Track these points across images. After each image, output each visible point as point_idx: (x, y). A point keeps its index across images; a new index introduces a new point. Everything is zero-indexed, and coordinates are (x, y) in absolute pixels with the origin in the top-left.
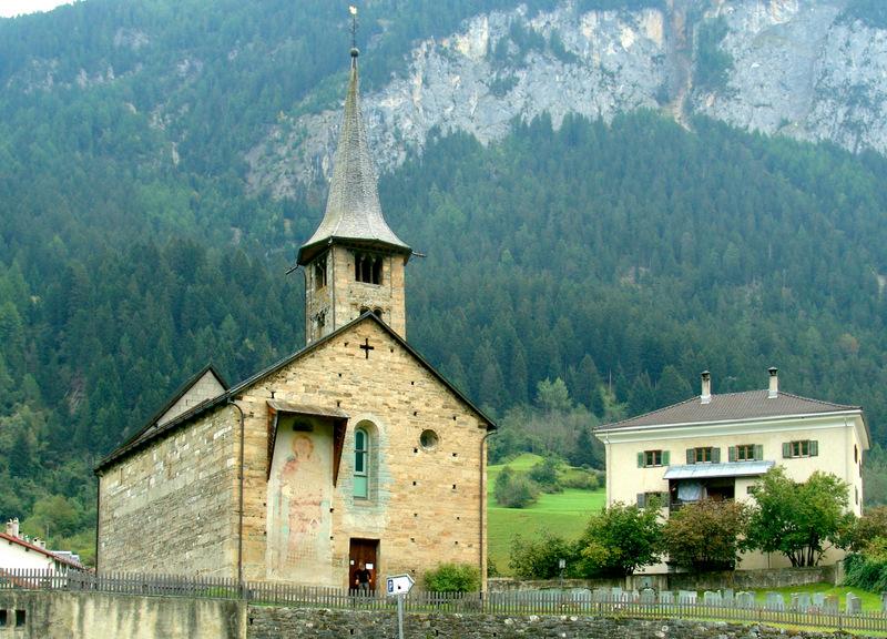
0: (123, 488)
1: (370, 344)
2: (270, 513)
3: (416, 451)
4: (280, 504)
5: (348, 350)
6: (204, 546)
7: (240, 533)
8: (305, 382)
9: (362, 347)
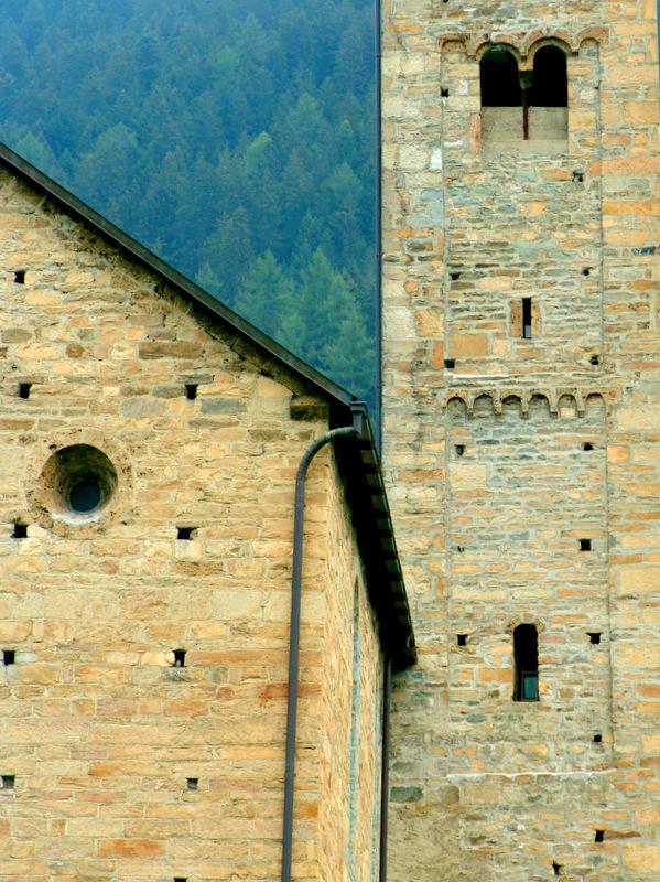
3: (20, 531)
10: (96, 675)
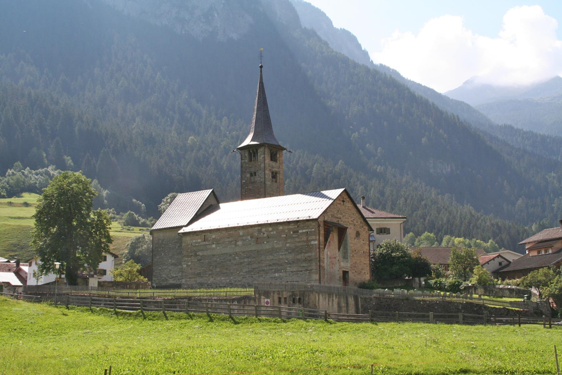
0: (207, 243)
7: (320, 269)
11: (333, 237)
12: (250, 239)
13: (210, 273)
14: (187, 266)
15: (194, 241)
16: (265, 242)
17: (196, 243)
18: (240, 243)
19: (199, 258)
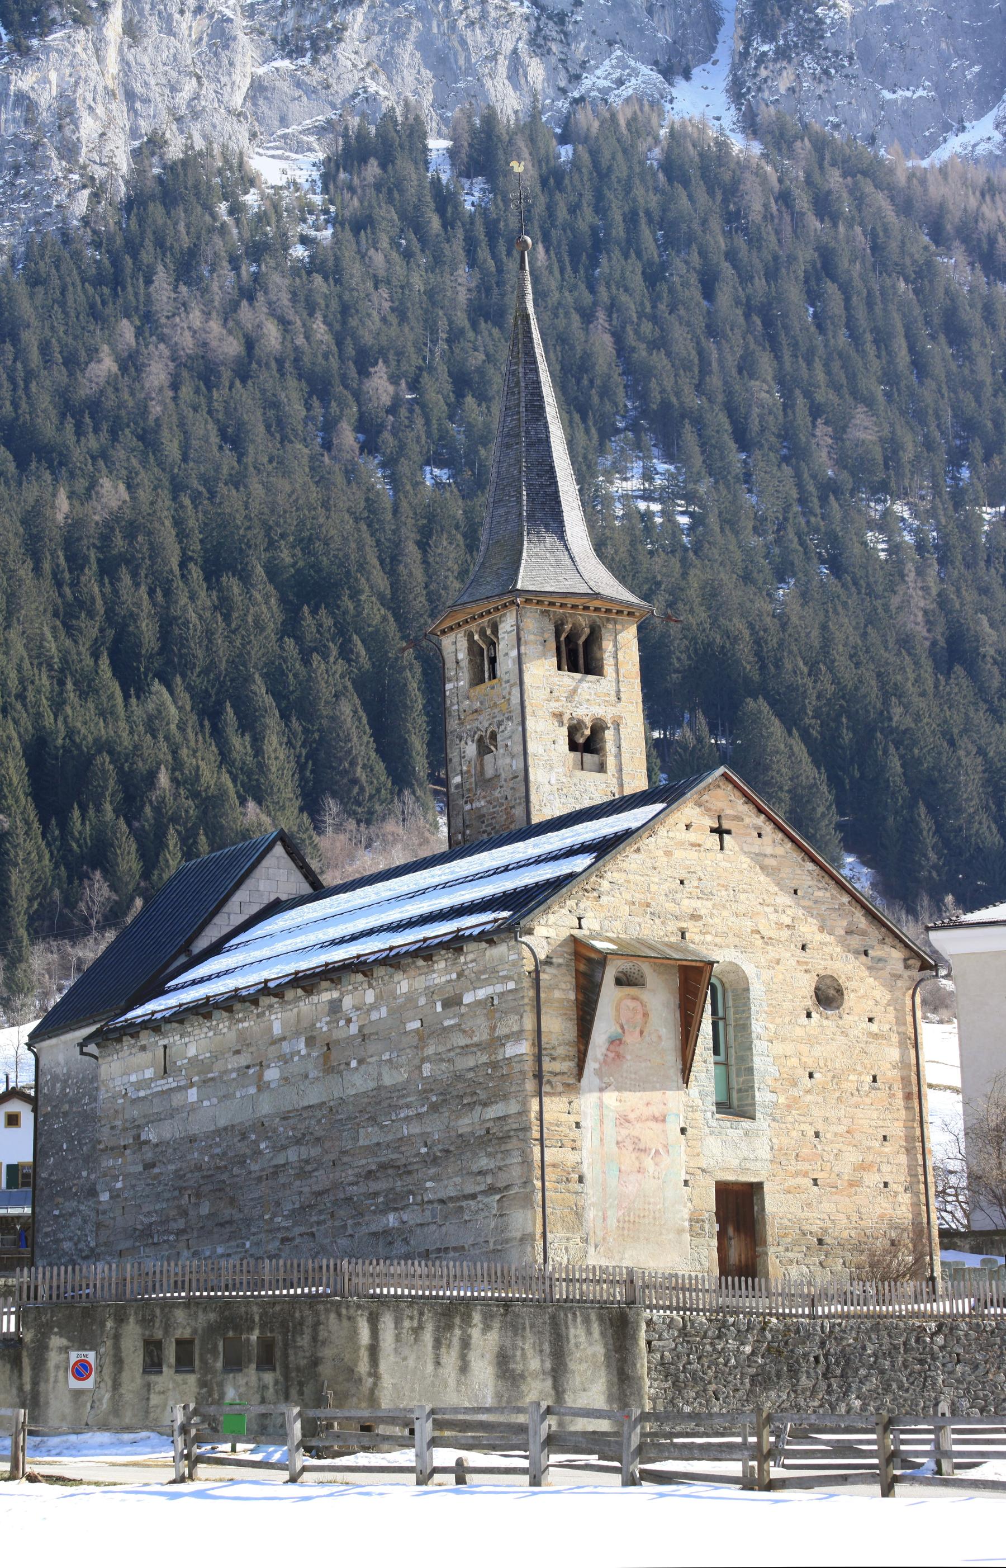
0: (171, 1082)
1: (726, 825)
2: (588, 1141)
3: (809, 1015)
4: (601, 1122)
5: (691, 836)
6: (442, 1201)
8: (629, 897)
9: (713, 830)
10: (844, 1086)
11: (646, 1015)
12: (304, 1052)
13: (181, 1224)
14: (111, 1197)
15: (133, 1078)
16: (354, 1064)
17: (139, 1085)
18: (272, 1074)
19: (149, 1156)
